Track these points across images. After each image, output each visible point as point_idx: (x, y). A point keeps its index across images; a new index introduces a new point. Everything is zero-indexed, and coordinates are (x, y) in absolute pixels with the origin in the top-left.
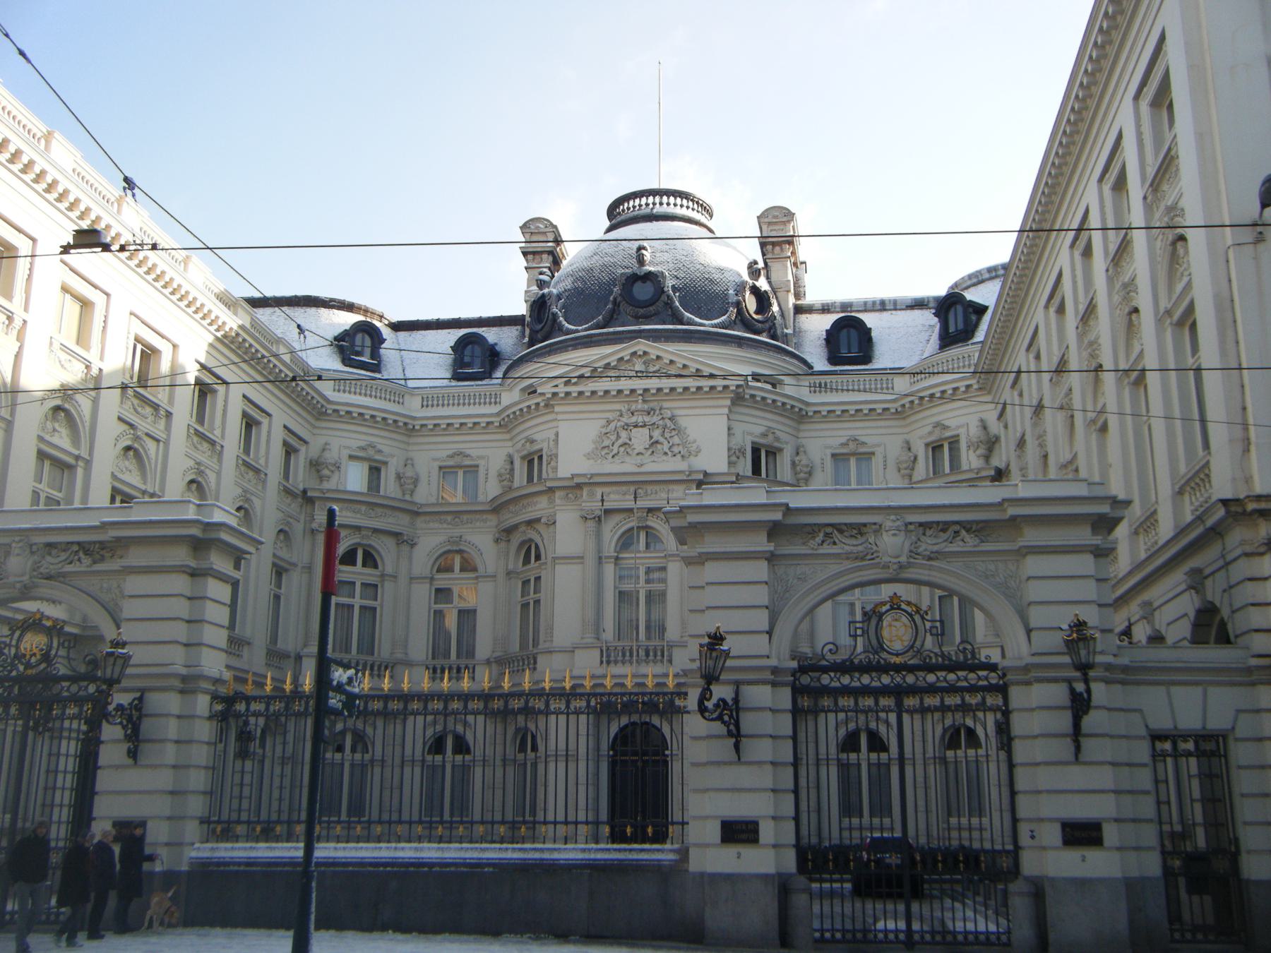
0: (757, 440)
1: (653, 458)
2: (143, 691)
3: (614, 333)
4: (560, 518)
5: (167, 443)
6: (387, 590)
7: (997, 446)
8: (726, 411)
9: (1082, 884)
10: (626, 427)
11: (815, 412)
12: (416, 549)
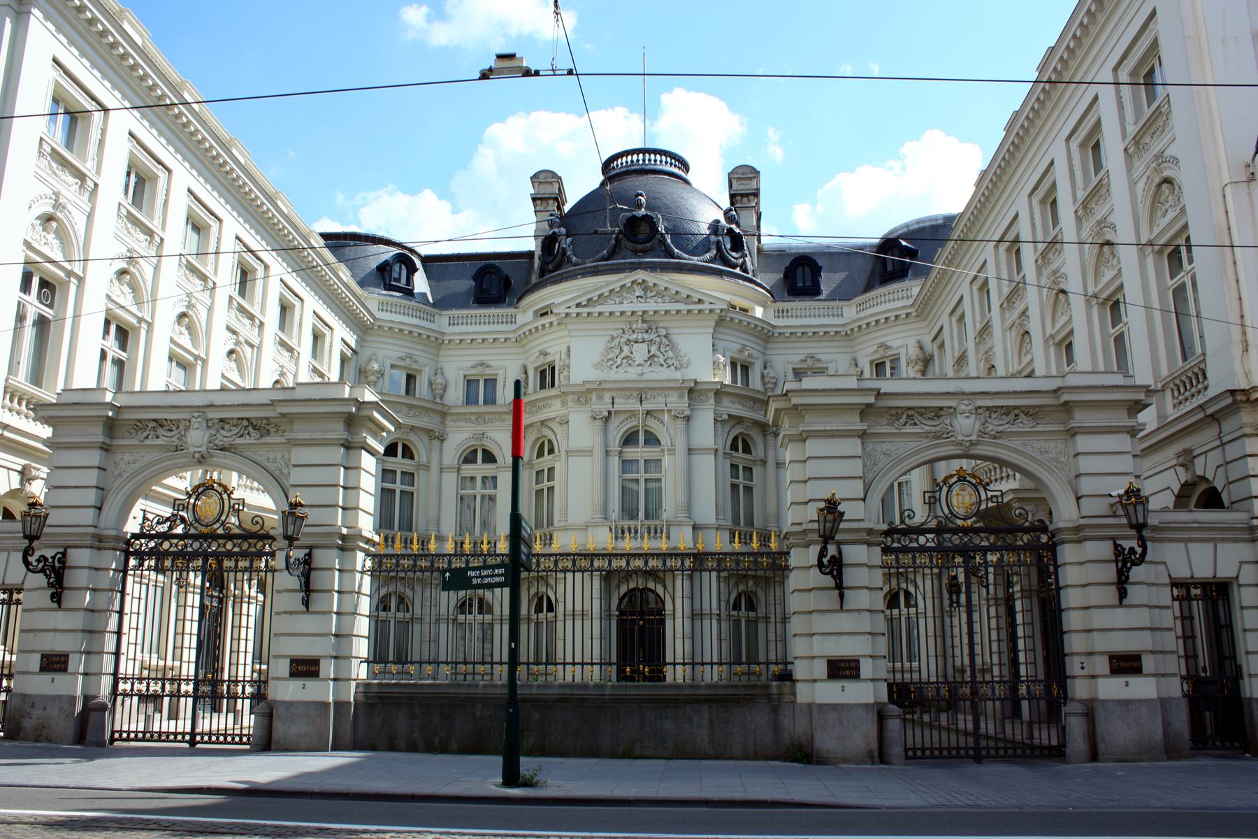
2: (311, 548)
4: (572, 418)
5: (260, 348)
6: (420, 478)
9: (1126, 704)
12: (446, 444)
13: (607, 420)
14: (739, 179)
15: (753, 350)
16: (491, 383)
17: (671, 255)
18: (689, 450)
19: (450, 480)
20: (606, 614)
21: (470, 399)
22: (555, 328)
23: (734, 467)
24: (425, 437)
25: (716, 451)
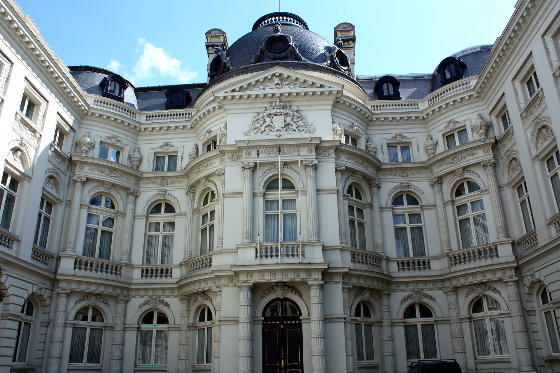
0: (346, 128)
1: (286, 132)
3: (261, 65)
7: (491, 128)
8: (330, 107)
10: (270, 115)
11: (377, 119)
12: (139, 199)
13: (254, 169)
14: (341, 31)
15: (358, 127)
16: (173, 158)
17: (299, 59)
18: (318, 190)
19: (140, 225)
20: (253, 321)
21: (158, 167)
22: (217, 111)
23: (351, 208)
24: (123, 194)
25: (338, 191)
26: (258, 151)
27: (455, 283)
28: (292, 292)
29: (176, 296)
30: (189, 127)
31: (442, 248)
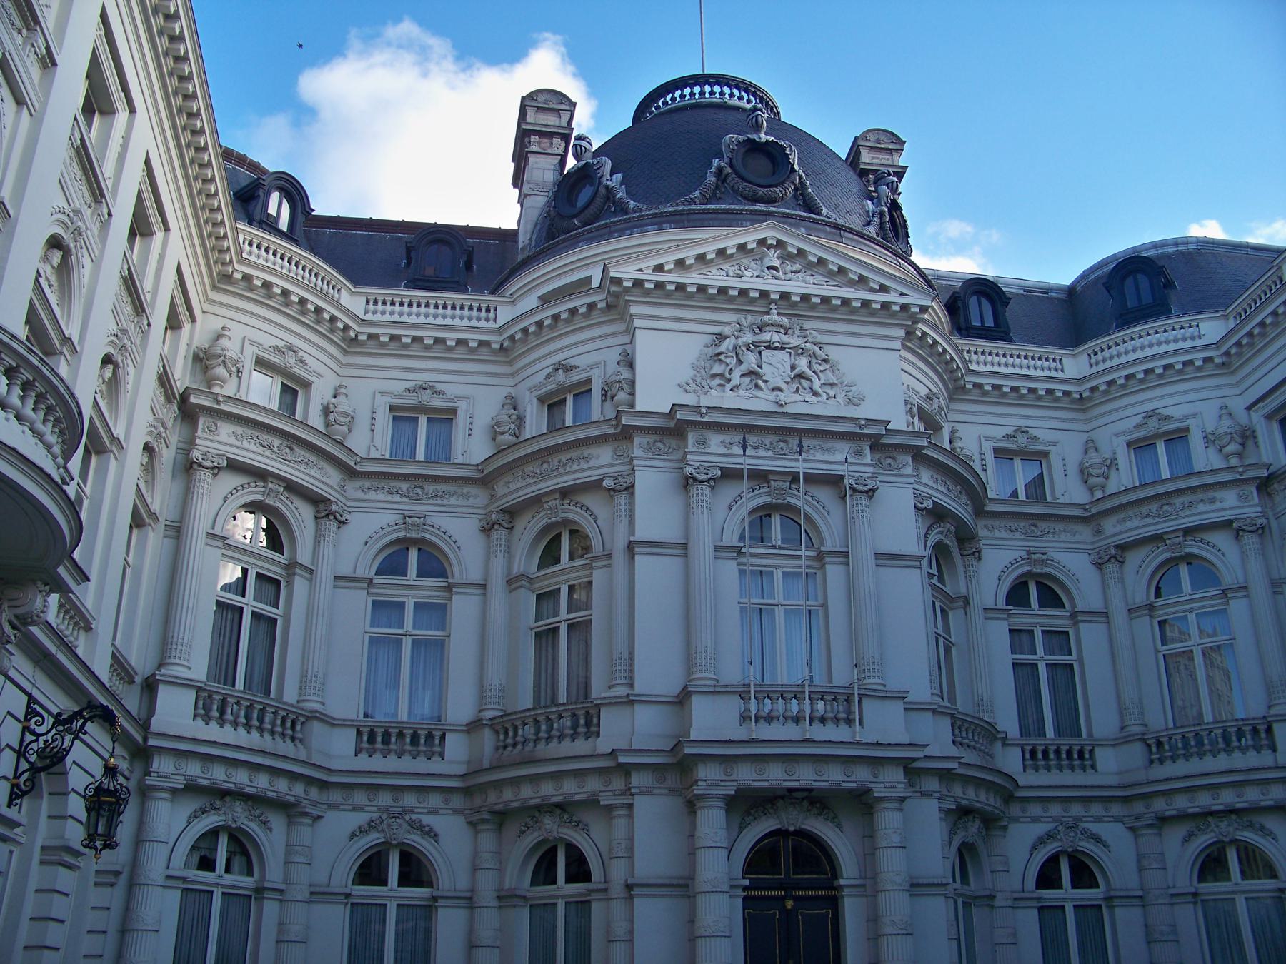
7: (1250, 443)
10: (756, 347)
22: (597, 317)
26: (744, 440)
27: (1159, 805)
28: (820, 814)
29: (456, 812)
30: (496, 346)
31: (1122, 721)
